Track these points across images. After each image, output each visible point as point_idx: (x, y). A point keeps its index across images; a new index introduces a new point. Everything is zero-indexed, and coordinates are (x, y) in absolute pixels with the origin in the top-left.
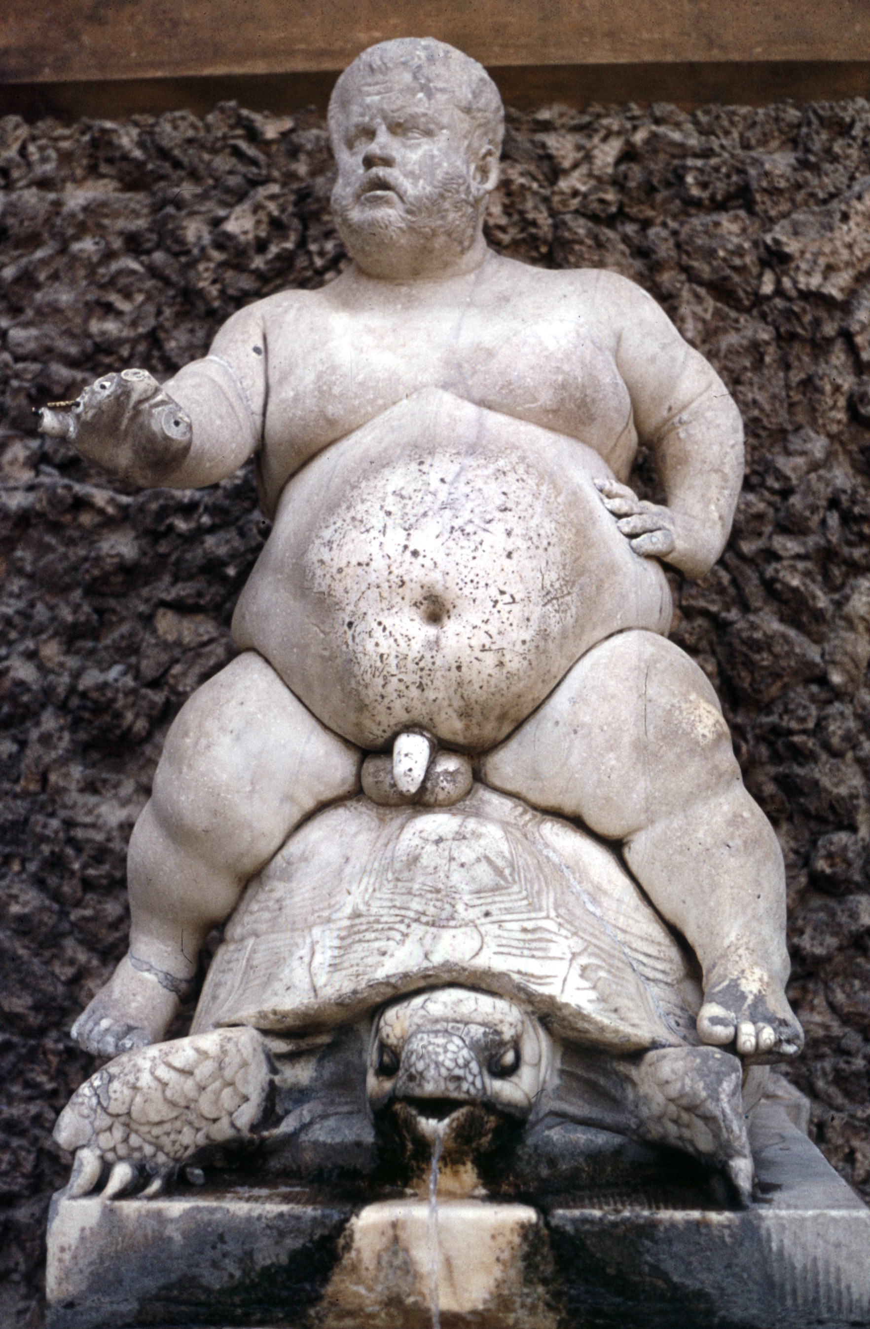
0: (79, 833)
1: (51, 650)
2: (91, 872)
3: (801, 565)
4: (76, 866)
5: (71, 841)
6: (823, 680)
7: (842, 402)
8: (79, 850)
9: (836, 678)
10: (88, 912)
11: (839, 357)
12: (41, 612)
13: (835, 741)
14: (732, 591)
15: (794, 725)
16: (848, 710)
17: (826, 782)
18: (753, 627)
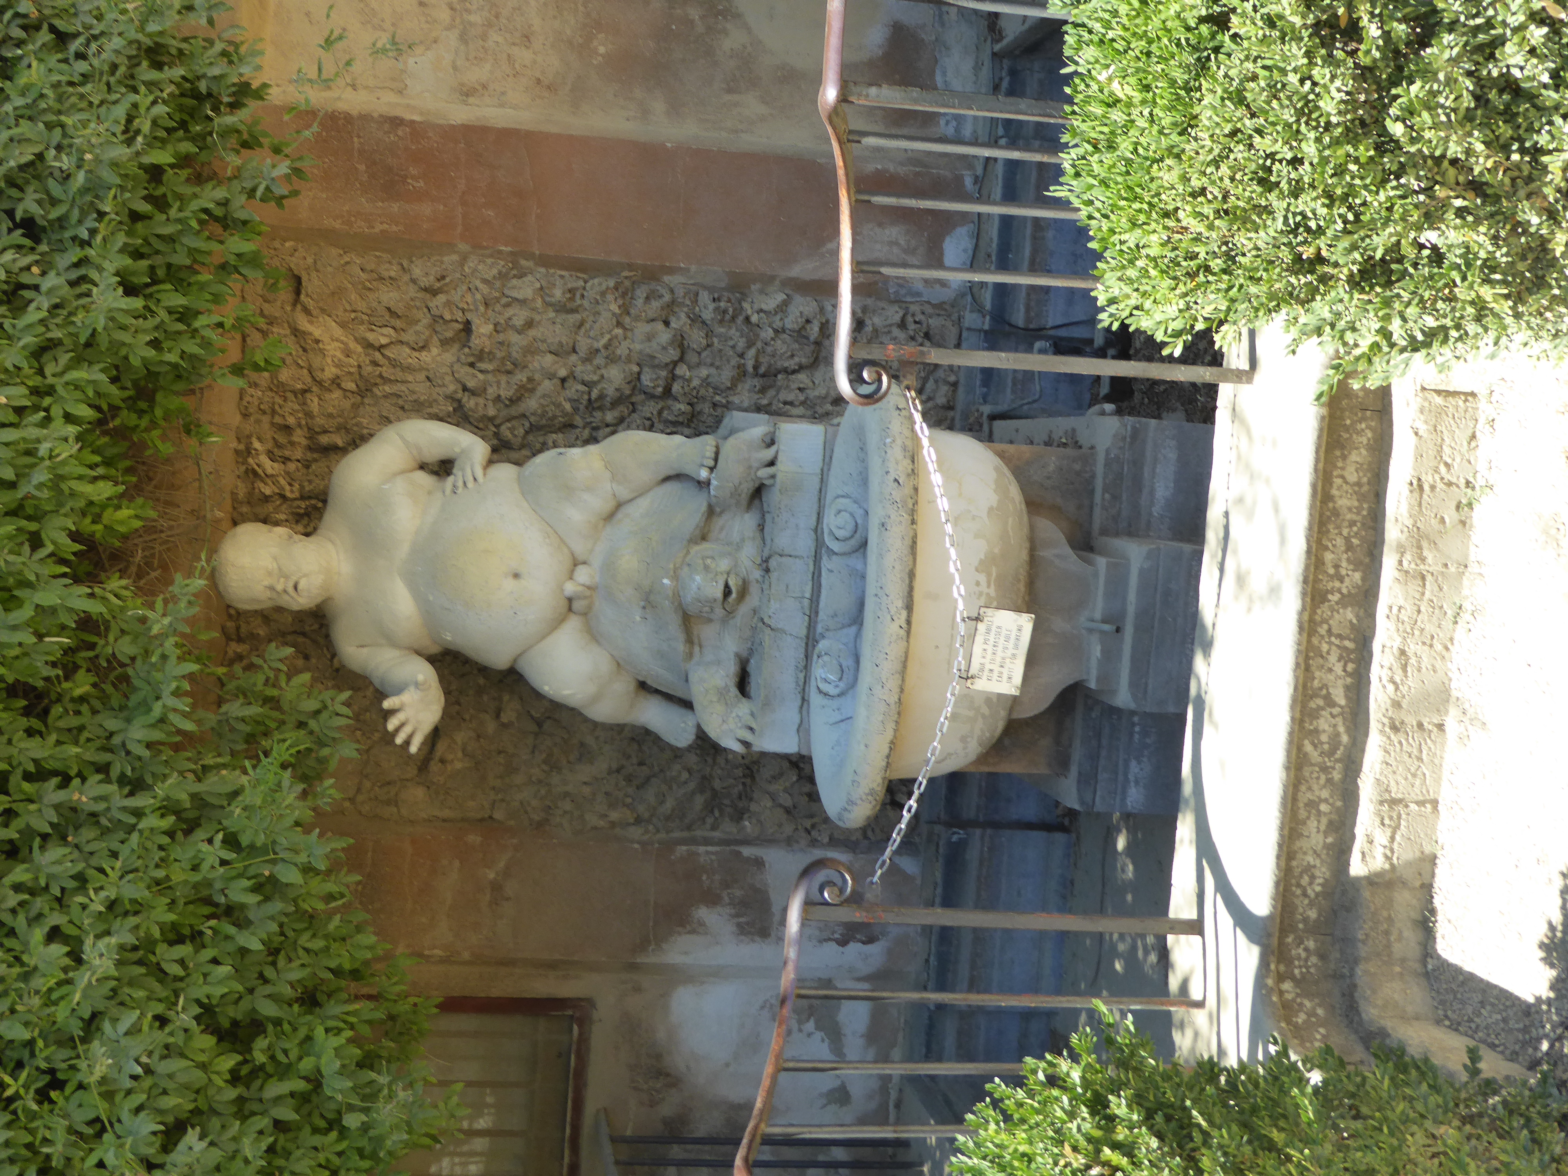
0: (614, 766)
2: (635, 760)
3: (503, 384)
5: (618, 771)
6: (563, 380)
7: (416, 354)
9: (563, 373)
14: (514, 422)
15: (586, 397)
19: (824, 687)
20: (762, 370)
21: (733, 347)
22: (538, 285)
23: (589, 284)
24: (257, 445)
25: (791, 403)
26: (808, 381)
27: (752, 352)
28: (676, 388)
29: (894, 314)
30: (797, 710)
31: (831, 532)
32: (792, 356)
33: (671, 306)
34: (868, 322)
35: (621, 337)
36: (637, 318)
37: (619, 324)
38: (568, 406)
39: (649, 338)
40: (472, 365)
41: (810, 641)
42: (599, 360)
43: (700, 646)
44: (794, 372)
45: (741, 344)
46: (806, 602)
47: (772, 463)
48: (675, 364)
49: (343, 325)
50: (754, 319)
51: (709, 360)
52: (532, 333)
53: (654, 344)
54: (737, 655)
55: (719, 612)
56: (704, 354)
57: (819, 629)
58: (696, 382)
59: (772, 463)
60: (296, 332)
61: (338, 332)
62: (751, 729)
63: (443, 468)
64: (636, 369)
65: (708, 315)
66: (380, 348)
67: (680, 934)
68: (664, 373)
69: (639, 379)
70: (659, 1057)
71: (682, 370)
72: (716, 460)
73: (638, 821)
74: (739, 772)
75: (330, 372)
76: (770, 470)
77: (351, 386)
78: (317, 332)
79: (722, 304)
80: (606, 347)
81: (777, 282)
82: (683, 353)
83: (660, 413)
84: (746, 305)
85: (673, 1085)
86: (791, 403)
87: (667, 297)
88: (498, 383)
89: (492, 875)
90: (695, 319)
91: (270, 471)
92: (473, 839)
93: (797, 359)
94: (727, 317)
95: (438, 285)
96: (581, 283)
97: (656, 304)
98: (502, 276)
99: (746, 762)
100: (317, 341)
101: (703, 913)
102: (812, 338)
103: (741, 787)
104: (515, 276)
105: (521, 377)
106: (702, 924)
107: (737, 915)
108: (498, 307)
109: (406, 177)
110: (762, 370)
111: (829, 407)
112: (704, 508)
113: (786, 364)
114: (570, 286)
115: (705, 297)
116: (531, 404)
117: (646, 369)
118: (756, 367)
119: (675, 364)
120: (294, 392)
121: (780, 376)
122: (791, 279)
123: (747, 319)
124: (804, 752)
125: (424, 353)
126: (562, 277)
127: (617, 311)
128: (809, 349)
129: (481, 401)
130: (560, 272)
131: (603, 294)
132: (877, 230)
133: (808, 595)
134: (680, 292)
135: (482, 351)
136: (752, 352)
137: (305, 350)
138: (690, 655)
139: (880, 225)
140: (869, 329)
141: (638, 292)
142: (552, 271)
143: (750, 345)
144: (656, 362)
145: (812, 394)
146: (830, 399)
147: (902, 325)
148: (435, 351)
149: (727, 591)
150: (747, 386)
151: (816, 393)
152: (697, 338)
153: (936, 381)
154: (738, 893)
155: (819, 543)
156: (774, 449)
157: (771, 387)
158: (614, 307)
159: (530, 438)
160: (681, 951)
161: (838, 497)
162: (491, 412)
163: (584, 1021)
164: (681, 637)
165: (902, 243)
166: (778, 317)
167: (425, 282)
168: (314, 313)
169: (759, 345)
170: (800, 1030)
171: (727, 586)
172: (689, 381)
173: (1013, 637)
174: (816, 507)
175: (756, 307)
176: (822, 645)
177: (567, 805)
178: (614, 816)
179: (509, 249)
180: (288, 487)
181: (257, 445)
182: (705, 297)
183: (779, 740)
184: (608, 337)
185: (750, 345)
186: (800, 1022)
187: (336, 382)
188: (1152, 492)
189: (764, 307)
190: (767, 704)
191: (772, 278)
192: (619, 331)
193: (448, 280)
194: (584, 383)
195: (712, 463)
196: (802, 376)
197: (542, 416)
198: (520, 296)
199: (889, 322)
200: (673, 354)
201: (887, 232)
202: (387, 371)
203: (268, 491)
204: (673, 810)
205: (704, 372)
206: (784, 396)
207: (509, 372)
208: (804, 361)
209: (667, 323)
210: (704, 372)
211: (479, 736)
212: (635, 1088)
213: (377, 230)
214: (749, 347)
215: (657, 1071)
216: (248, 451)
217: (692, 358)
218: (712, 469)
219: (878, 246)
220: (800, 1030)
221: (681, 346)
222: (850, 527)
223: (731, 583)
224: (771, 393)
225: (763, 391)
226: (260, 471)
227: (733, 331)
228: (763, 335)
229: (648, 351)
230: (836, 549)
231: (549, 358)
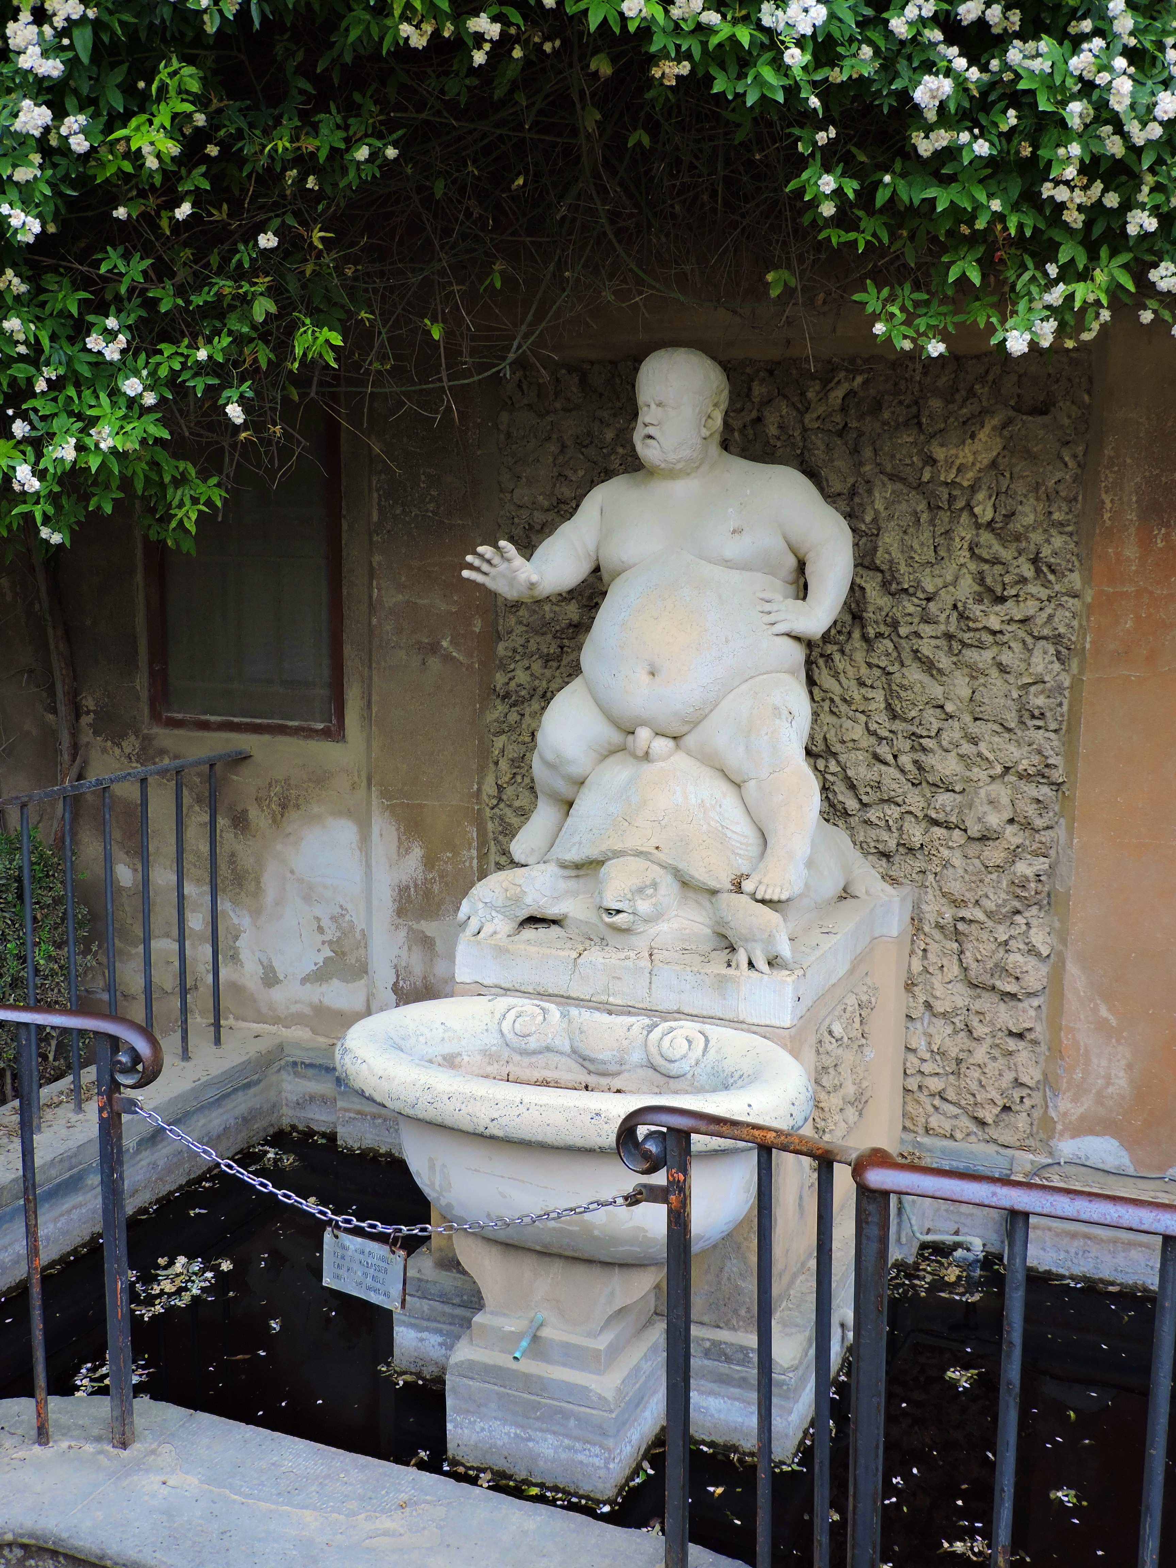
1: (537, 667)
3: (934, 642)
7: (966, 546)
9: (949, 708)
11: (965, 518)
12: (532, 646)
13: (944, 743)
14: (895, 654)
15: (925, 733)
16: (956, 725)
17: (938, 767)
18: (904, 676)
20: (961, 926)
22: (1046, 679)
23: (1052, 735)
24: (859, 380)
25: (925, 957)
26: (950, 976)
27: (980, 915)
28: (938, 831)
29: (1031, 1075)
33: (1027, 826)
34: (1021, 1044)
35: (992, 772)
36: (1015, 788)
37: (1007, 769)
38: (913, 713)
40: (955, 607)
41: (565, 999)
42: (967, 748)
44: (960, 960)
45: (990, 905)
46: (604, 998)
47: (751, 964)
48: (965, 831)
49: (994, 464)
50: (1018, 919)
51: (970, 868)
52: (994, 673)
53: (986, 808)
54: (565, 916)
56: (977, 862)
57: (574, 1012)
59: (751, 964)
60: (985, 412)
61: (985, 459)
63: (801, 585)
65: (1022, 868)
66: (969, 507)
67: (398, 829)
70: (297, 806)
72: (763, 901)
73: (500, 788)
75: (940, 453)
77: (926, 477)
78: (982, 435)
79: (1033, 885)
80: (980, 755)
81: (1061, 947)
83: (911, 813)
84: (1034, 910)
85: (274, 821)
86: (925, 957)
87: (1039, 823)
88: (937, 637)
89: (445, 644)
90: (1015, 853)
91: (832, 395)
92: (477, 626)
93: (974, 965)
94: (1019, 891)
95: (1045, 569)
96: (1053, 726)
97: (1031, 810)
98: (1057, 639)
100: (973, 436)
101: (417, 852)
102: (998, 983)
104: (1058, 653)
105: (944, 662)
106: (408, 851)
107: (416, 885)
108: (1021, 634)
109: (1168, 526)
110: (961, 926)
111: (921, 999)
112: (713, 884)
113: (968, 954)
114: (1048, 714)
115: (1041, 864)
116: (914, 674)
120: (917, 416)
121: (955, 945)
122: (1064, 963)
123: (1018, 912)
125: (967, 554)
126: (1060, 705)
127: (1021, 768)
129: (916, 620)
130: (1066, 702)
131: (1039, 752)
132: (1123, 1062)
133: (611, 1000)
134: (1045, 836)
135: (968, 618)
137: (964, 423)
138: (563, 866)
139: (1130, 1067)
140: (1012, 1044)
141: (1045, 789)
142: (1066, 693)
143: (989, 915)
145: (937, 981)
146: (931, 1000)
147: (1018, 1083)
148: (973, 566)
151: (937, 985)
152: (994, 854)
153: (956, 1117)
154: (436, 888)
156: (765, 968)
157: (945, 936)
158: (1024, 765)
159: (877, 672)
160: (384, 831)
161: (707, 1041)
162: (903, 631)
163: (326, 734)
165: (1110, 1090)
166: (1022, 946)
167: (1046, 552)
168: (1005, 433)
169: (990, 924)
170: (323, 943)
171: (618, 912)
173: (378, 1286)
174: (705, 1013)
175: (1034, 922)
177: (513, 717)
178: (504, 764)
179: (1088, 646)
180: (815, 415)
181: (859, 380)
182: (1041, 864)
184: (991, 757)
185: (989, 915)
186: (330, 942)
187: (931, 461)
188: (712, 1393)
189: (1033, 931)
190: (500, 951)
191: (1064, 941)
192: (999, 769)
193: (1051, 577)
194: (940, 730)
195: (759, 897)
196: (956, 970)
197: (901, 686)
198: (1034, 660)
199: (1021, 1068)
201: (1122, 1074)
202: (945, 516)
203: (810, 395)
204: (510, 825)
205: (957, 861)
206: (933, 948)
207: (950, 647)
208: (972, 974)
209: (1011, 821)
210: (957, 861)
211: (575, 626)
212: (270, 784)
213: (1104, 496)
214: (985, 912)
215: (286, 804)
216: (853, 372)
217: (974, 849)
218: (753, 896)
219: (1104, 1063)
220: (323, 943)
222: (670, 1054)
223: (621, 915)
224: (938, 936)
225: (940, 927)
226: (832, 384)
227: (1003, 896)
228: (1001, 929)
230: (652, 1035)
231: (966, 692)
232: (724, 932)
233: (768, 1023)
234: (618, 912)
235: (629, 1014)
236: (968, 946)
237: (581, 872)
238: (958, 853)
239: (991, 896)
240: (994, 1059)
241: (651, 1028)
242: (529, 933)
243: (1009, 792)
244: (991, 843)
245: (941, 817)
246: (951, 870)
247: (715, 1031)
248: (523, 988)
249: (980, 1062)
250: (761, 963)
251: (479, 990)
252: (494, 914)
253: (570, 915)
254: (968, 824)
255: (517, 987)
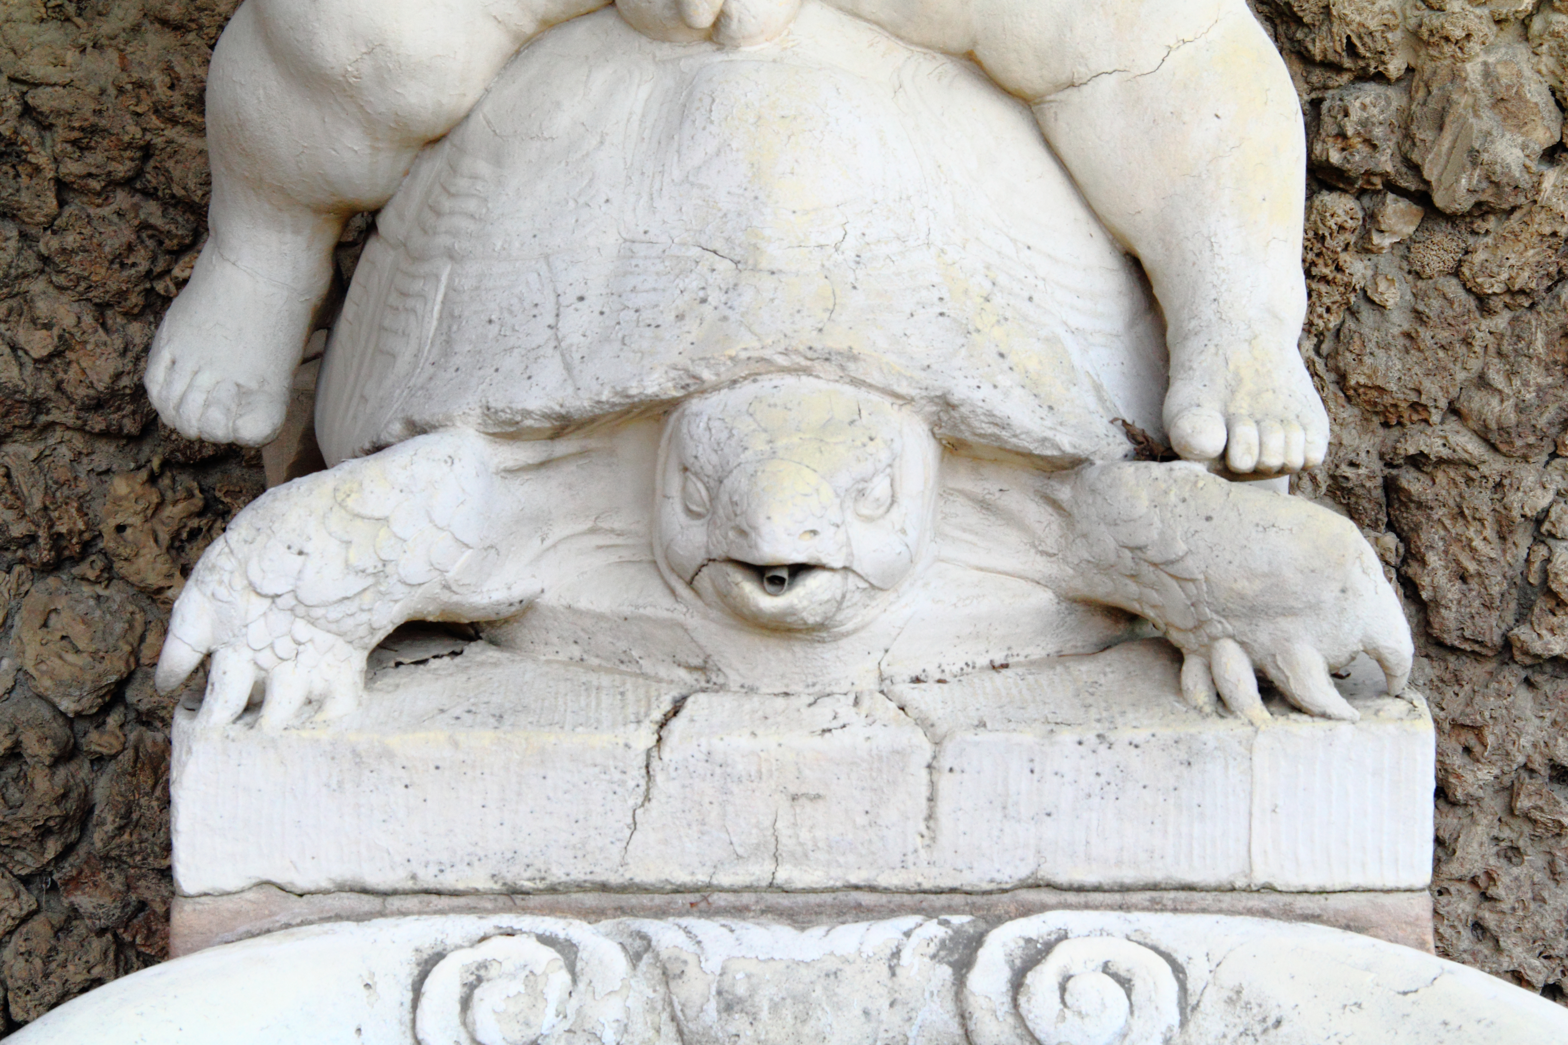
0: (42, 99)
2: (72, 168)
4: (42, 158)
5: (28, 111)
8: (44, 126)
10: (71, 240)
19: (445, 983)
21: (1482, 382)
30: (346, 872)
31: (1035, 954)
32: (1463, 578)
39: (1505, 103)
41: (611, 898)
43: (542, 465)
45: (1494, 409)
46: (758, 871)
47: (1270, 691)
48: (1422, 197)
53: (1487, 120)
55: (691, 539)
56: (1453, 287)
57: (666, 934)
58: (1358, 269)
59: (1270, 691)
62: (253, 705)
64: (1395, 67)
68: (1386, 162)
69: (1363, 77)
71: (1398, 218)
74: (68, 522)
76: (1245, 689)
82: (1452, 218)
93: (1452, 591)
99: (108, 542)
102: (1523, 633)
103: (18, 530)
110: (1412, 482)
112: (1068, 442)
113: (1433, 559)
117: (1396, 97)
118: (1418, 461)
119: (1422, 197)
124: (184, 917)
128: (1491, 628)
136: (1469, 445)
138: (507, 429)
144: (1423, 134)
149: (776, 576)
150: (1351, 438)
155: (991, 905)
164: (578, 402)
169: (1494, 466)
171: (799, 570)
172: (1365, 249)
176: (599, 942)
183: (223, 814)
200: (1456, 190)
210: (1393, 294)
214: (1484, 435)
218: (1223, 467)
221: (1482, 210)
223: (812, 583)
227: (1537, 376)
228: (1529, 475)
229: (1465, 100)
232: (1127, 595)
233: (1355, 880)
234: (799, 570)
235: (862, 913)
236: (1431, 537)
237: (562, 447)
238: (1388, 264)
239: (1497, 379)
240: (1512, 854)
241: (962, 955)
242: (435, 682)
243: (1547, 62)
244: (1491, 223)
245: (1359, 160)
246: (1367, 314)
247: (1187, 932)
248: (449, 881)
249: (1478, 869)
250: (1314, 685)
251: (278, 907)
252: (302, 630)
253: (549, 599)
254: (1430, 173)
255: (428, 879)
